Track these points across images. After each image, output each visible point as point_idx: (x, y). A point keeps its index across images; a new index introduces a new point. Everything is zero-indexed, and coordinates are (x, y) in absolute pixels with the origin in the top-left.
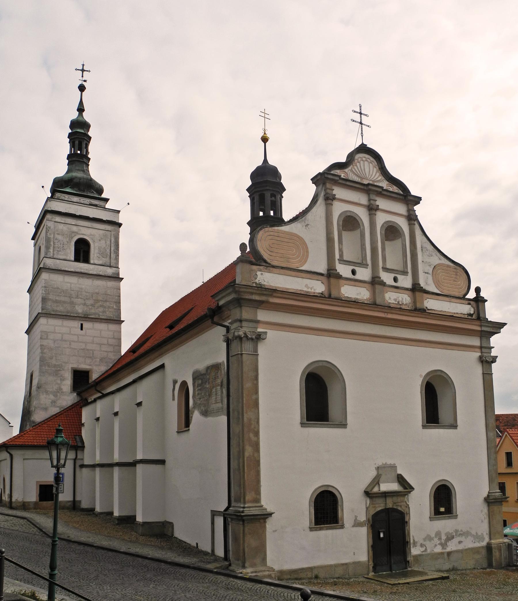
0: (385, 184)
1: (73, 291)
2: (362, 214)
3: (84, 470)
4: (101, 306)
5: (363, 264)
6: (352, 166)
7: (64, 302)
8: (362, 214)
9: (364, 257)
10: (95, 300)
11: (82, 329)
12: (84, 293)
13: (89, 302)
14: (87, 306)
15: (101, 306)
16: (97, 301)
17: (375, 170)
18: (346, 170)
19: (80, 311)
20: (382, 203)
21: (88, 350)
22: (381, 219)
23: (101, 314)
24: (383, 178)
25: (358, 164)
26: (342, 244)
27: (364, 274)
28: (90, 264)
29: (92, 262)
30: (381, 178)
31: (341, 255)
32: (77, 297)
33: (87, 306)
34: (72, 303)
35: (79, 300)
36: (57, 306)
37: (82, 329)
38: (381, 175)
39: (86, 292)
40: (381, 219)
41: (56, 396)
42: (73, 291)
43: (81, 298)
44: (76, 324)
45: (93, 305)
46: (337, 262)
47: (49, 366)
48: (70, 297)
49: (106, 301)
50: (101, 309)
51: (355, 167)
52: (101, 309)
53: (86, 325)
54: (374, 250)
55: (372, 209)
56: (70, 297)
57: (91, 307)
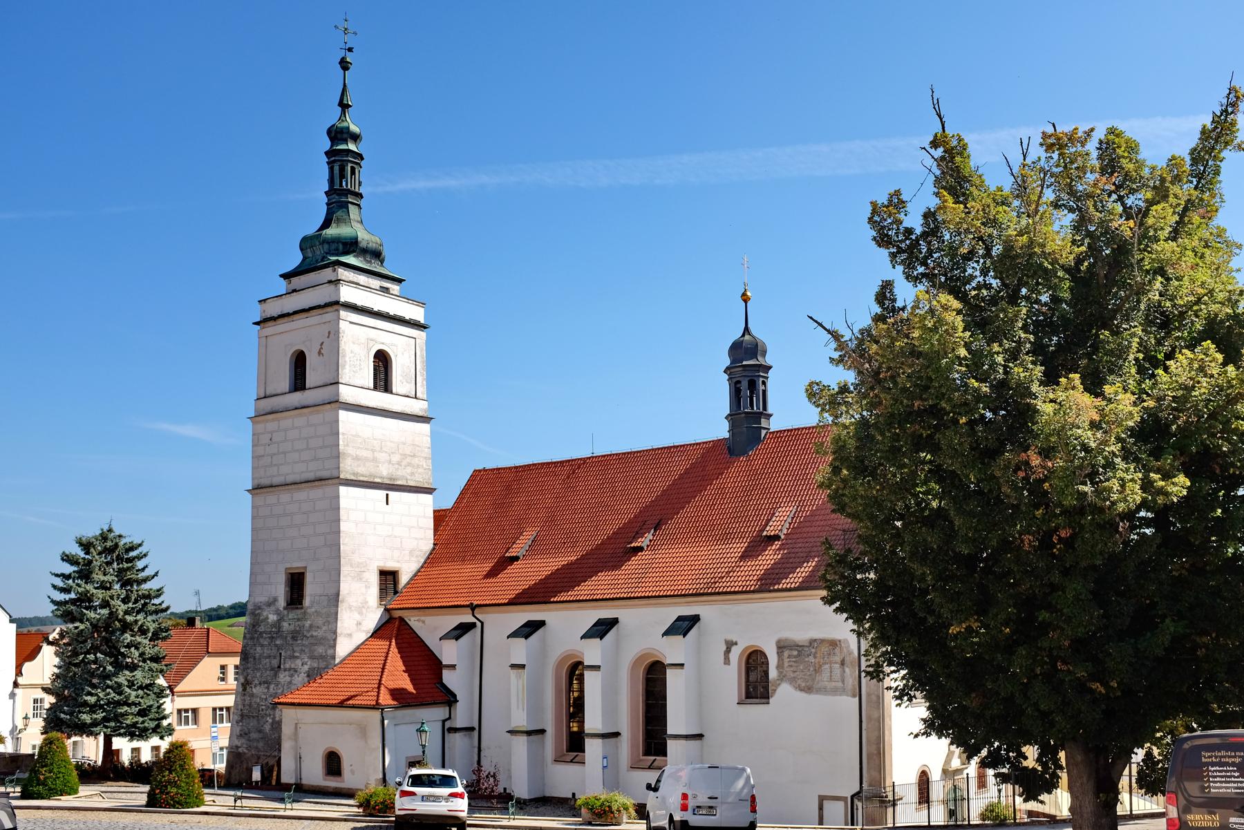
1: (375, 439)
3: (458, 735)
4: (409, 464)
7: (367, 459)
10: (401, 454)
11: (387, 504)
12: (388, 443)
13: (396, 458)
14: (393, 464)
15: (409, 464)
16: (405, 456)
19: (385, 473)
21: (396, 537)
23: (409, 477)
28: (391, 393)
29: (394, 391)
32: (381, 451)
33: (393, 464)
34: (375, 460)
35: (384, 454)
36: (359, 466)
37: (387, 504)
39: (391, 442)
41: (360, 613)
42: (375, 439)
43: (386, 452)
44: (381, 494)
45: (399, 463)
47: (351, 566)
48: (373, 451)
49: (414, 456)
50: (409, 470)
52: (409, 470)
53: (392, 494)
56: (373, 451)
57: (397, 466)
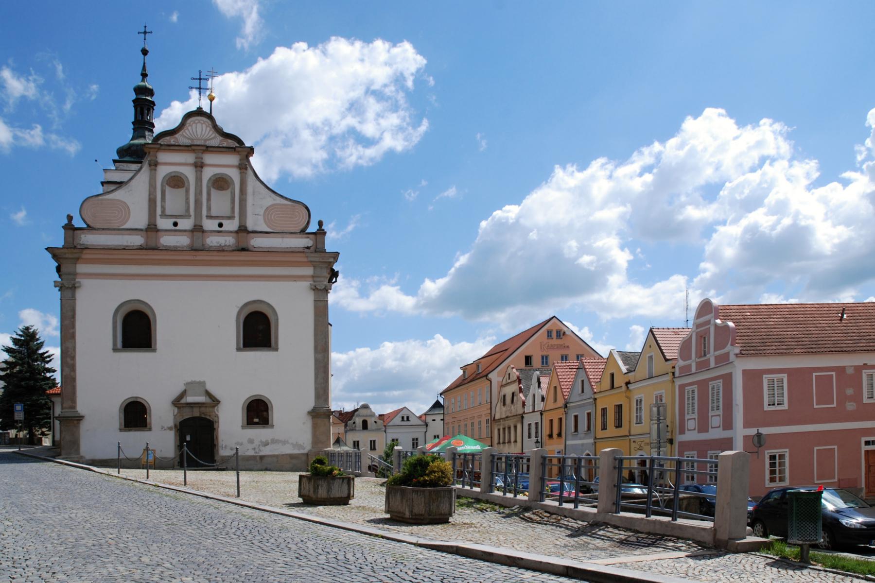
0: (217, 141)
2: (189, 173)
5: (186, 216)
6: (183, 131)
8: (189, 173)
9: (188, 210)
17: (208, 129)
18: (177, 136)
20: (209, 159)
22: (208, 173)
24: (217, 135)
25: (190, 128)
26: (165, 202)
27: (186, 224)
30: (215, 134)
31: (163, 210)
38: (215, 132)
40: (208, 173)
46: (158, 217)
51: (187, 131)
54: (198, 203)
55: (199, 166)
